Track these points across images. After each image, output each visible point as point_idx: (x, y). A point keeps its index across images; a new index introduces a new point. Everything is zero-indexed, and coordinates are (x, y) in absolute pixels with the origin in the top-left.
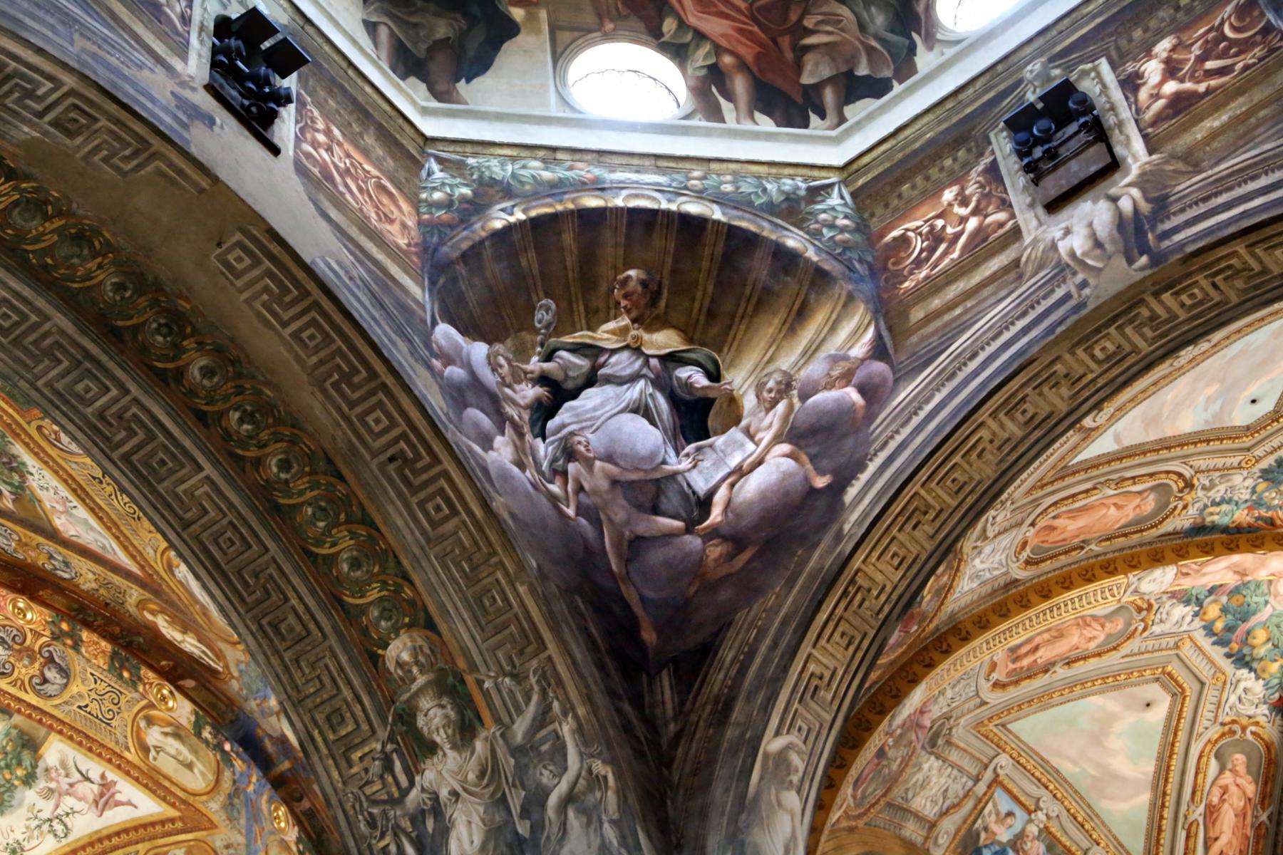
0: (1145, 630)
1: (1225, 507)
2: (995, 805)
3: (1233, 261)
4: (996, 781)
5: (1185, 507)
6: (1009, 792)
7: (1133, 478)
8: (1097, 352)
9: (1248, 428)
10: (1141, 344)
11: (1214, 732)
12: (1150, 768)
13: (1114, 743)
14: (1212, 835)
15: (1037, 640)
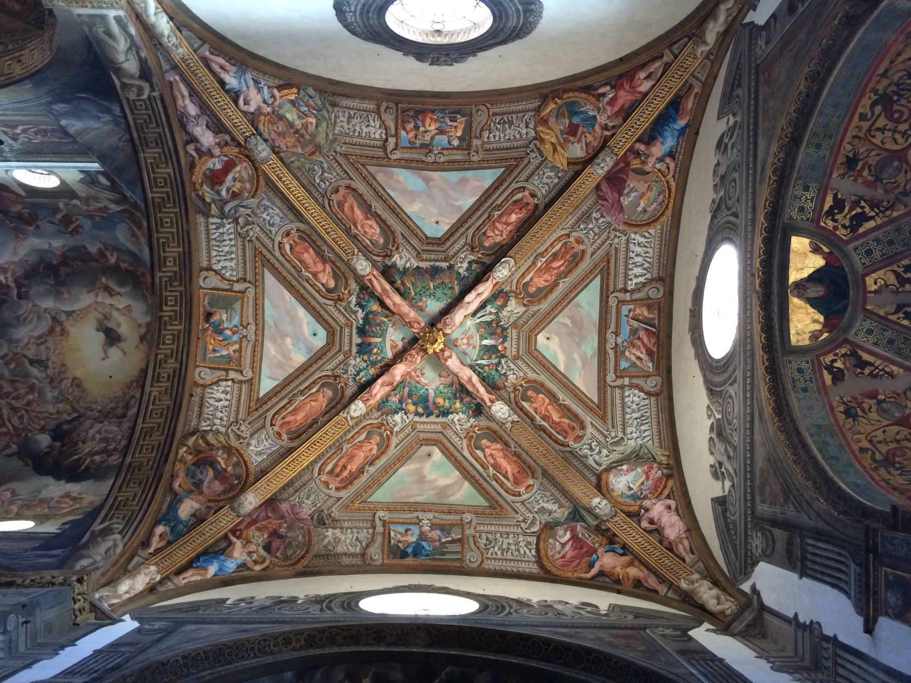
0: (392, 433)
1: (362, 374)
2: (395, 531)
3: (164, 279)
4: (384, 523)
5: (346, 384)
6: (398, 523)
7: (306, 388)
8: (167, 342)
9: (327, 344)
10: (178, 327)
11: (465, 442)
12: (457, 473)
13: (431, 477)
14: (504, 472)
15: (341, 464)
